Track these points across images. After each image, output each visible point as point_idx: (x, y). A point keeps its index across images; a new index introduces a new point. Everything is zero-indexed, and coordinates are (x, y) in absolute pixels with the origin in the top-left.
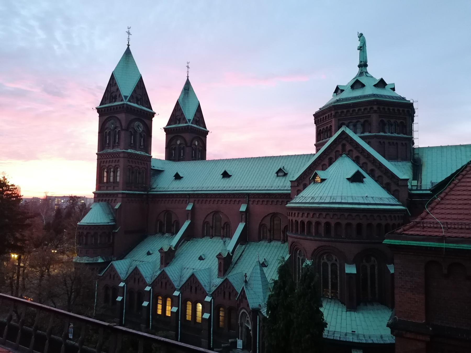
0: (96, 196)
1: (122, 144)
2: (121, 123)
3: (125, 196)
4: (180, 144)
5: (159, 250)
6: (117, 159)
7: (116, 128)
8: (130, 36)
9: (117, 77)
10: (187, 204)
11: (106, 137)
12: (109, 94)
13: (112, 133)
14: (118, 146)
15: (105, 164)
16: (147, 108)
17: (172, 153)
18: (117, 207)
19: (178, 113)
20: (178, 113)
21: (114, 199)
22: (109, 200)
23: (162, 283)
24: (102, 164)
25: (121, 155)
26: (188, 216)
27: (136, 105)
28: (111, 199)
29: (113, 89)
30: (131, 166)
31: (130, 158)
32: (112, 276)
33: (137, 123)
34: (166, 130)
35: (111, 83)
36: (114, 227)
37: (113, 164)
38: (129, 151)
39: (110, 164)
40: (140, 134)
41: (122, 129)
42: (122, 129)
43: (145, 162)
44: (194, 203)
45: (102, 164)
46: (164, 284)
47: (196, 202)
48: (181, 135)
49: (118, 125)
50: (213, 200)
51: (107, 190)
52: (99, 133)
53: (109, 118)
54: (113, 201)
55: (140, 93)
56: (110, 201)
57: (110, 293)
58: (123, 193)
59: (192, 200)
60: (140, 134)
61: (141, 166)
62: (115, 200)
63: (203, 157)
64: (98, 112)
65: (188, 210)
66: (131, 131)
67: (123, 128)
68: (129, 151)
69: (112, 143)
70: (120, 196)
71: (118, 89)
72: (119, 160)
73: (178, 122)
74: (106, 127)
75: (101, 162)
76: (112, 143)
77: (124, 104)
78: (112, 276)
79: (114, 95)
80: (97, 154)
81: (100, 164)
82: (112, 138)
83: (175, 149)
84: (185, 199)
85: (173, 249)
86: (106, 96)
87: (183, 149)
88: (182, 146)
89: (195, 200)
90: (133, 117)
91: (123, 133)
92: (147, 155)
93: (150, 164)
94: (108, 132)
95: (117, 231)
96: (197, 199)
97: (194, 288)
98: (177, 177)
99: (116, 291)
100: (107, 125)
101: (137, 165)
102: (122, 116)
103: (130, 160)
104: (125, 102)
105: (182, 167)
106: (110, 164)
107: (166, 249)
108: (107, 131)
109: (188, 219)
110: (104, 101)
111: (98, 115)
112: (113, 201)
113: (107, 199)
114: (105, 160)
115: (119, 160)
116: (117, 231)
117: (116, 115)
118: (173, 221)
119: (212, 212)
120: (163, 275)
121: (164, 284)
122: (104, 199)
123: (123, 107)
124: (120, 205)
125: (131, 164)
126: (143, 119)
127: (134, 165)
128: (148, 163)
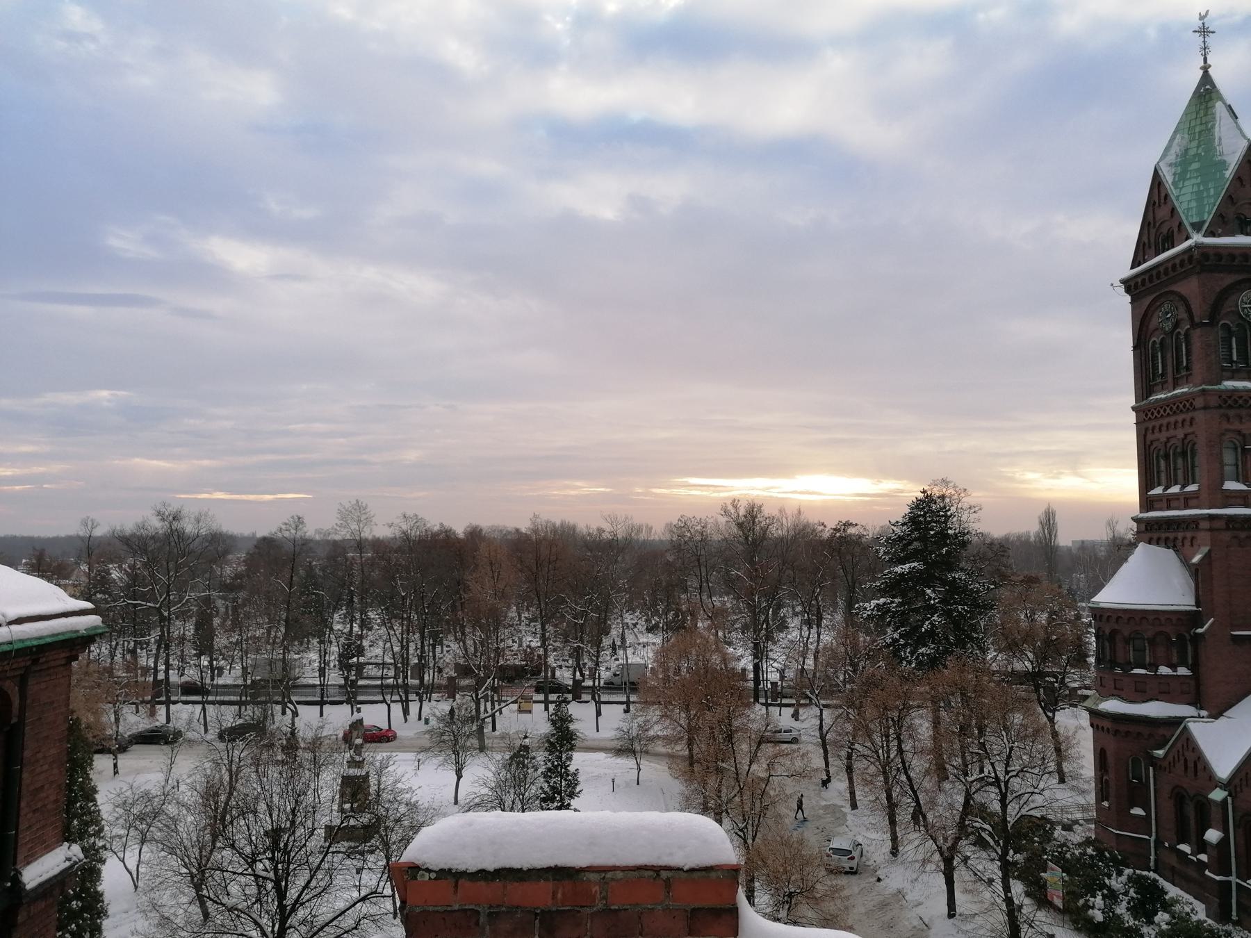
0: (1143, 527)
1: (1197, 368)
2: (1189, 310)
3: (1220, 524)
6: (1187, 416)
7: (1176, 325)
8: (1210, 40)
9: (1168, 177)
11: (1154, 357)
12: (1153, 231)
13: (1168, 341)
14: (1187, 376)
15: (1157, 435)
18: (1196, 559)
21: (1189, 535)
22: (1176, 538)
24: (1150, 437)
25: (1199, 402)
28: (1180, 535)
29: (1163, 213)
30: (1239, 432)
31: (1230, 407)
32: (1191, 765)
36: (1193, 618)
37: (1180, 433)
38: (1229, 384)
41: (1194, 325)
42: (1194, 325)
45: (1150, 437)
49: (1183, 315)
51: (1169, 508)
52: (1135, 348)
53: (1154, 300)
54: (1187, 543)
56: (1179, 543)
57: (1190, 811)
58: (1212, 518)
62: (1193, 538)
64: (1128, 291)
67: (1197, 320)
68: (1229, 384)
69: (1170, 370)
71: (1173, 210)
72: (1192, 419)
75: (1147, 429)
76: (1170, 370)
77: (1198, 246)
78: (1191, 765)
79: (1164, 230)
80: (1133, 408)
81: (1145, 436)
82: (1169, 355)
86: (1145, 239)
90: (1229, 279)
94: (1158, 341)
95: (1200, 630)
100: (1154, 322)
102: (1190, 287)
103: (1231, 413)
104: (1197, 238)
106: (1172, 432)
108: (1156, 339)
110: (1140, 258)
111: (1128, 298)
112: (1187, 543)
113: (1171, 535)
114: (1157, 424)
115: (1192, 419)
116: (1200, 630)
117: (1175, 288)
122: (1163, 535)
124: (1208, 556)
125: (1236, 425)
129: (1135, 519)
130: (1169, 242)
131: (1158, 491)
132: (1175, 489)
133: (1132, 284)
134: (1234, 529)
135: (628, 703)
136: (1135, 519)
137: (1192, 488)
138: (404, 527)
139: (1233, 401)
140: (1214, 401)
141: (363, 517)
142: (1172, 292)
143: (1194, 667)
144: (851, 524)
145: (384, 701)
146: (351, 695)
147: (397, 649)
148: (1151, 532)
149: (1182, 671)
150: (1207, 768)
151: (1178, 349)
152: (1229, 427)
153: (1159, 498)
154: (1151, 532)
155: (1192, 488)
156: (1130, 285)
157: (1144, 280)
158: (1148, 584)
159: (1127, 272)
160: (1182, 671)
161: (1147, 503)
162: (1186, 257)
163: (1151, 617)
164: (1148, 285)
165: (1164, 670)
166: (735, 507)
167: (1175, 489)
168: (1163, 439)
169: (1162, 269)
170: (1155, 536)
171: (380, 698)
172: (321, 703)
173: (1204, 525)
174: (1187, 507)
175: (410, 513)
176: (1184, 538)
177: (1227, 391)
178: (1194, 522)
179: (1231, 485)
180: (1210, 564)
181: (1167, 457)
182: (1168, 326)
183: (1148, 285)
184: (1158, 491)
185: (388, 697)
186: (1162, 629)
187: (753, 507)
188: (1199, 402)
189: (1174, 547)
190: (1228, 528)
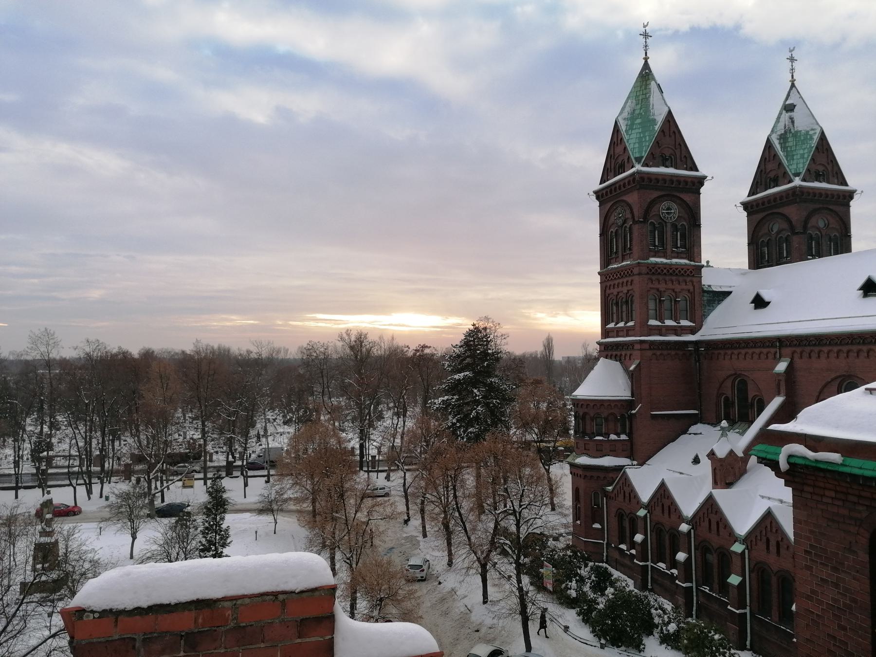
1: (636, 249)
3: (647, 346)
4: (778, 233)
5: (708, 456)
6: (630, 279)
7: (625, 222)
9: (623, 127)
10: (777, 361)
13: (620, 232)
15: (612, 290)
16: (686, 169)
17: (764, 252)
18: (632, 368)
19: (770, 166)
20: (770, 166)
21: (628, 353)
22: (621, 355)
23: (710, 521)
25: (636, 271)
26: (779, 385)
27: (671, 171)
28: (623, 353)
29: (619, 150)
30: (658, 290)
32: (627, 495)
33: (665, 204)
34: (746, 206)
35: (615, 140)
36: (629, 404)
37: (625, 289)
38: (653, 260)
39: (620, 289)
40: (675, 227)
41: (635, 222)
43: (688, 279)
44: (792, 359)
45: (608, 291)
46: (714, 526)
47: (796, 356)
48: (780, 210)
49: (629, 216)
50: (835, 349)
51: (618, 336)
52: (601, 235)
54: (628, 358)
55: (670, 143)
57: (627, 524)
58: (642, 342)
59: (787, 351)
60: (675, 227)
61: (678, 288)
63: (850, 251)
64: (598, 198)
65: (778, 374)
66: (652, 224)
67: (636, 219)
68: (653, 260)
69: (620, 250)
70: (637, 346)
71: (625, 148)
73: (772, 184)
74: (611, 222)
76: (620, 250)
78: (627, 495)
79: (620, 160)
80: (599, 273)
83: (768, 244)
84: (773, 350)
85: (740, 454)
87: (787, 240)
88: (784, 235)
89: (794, 353)
90: (656, 194)
91: (636, 228)
92: (692, 263)
93: (700, 281)
95: (633, 412)
96: (799, 350)
97: (773, 543)
98: (759, 302)
99: (634, 525)
100: (612, 219)
101: (670, 285)
102: (633, 198)
103: (654, 278)
104: (638, 167)
105: (777, 281)
106: (620, 289)
107: (721, 453)
108: (613, 230)
109: (779, 394)
111: (598, 203)
112: (628, 358)
113: (619, 353)
116: (633, 412)
118: (750, 397)
119: (840, 376)
120: (710, 504)
121: (714, 526)
122: (614, 353)
123: (634, 179)
124: (639, 365)
125: (656, 285)
126: (678, 194)
127: (662, 287)
128: (695, 279)
129: (598, 343)
130: (622, 168)
131: (612, 325)
132: (621, 324)
133: (600, 194)
134: (654, 349)
135: (268, 476)
136: (598, 343)
137: (631, 324)
138: (88, 350)
139: (655, 270)
140: (644, 270)
141: (51, 342)
142: (623, 201)
143: (630, 435)
144: (427, 347)
145: (71, 485)
146: (42, 481)
147: (81, 444)
148: (608, 350)
149: (623, 437)
150: (636, 496)
151: (625, 236)
152: (652, 286)
153: (612, 329)
154: (608, 350)
155: (631, 324)
156: (599, 195)
157: (607, 192)
158: (605, 383)
159: (597, 186)
160: (623, 437)
161: (606, 333)
162: (631, 179)
163: (606, 404)
164: (609, 195)
165: (613, 437)
166: (348, 335)
167: (621, 324)
168: (615, 293)
169: (617, 186)
170: (610, 353)
171: (67, 482)
172: (16, 489)
173: (637, 346)
174: (628, 335)
175: (92, 338)
176: (626, 355)
177: (652, 264)
178: (631, 344)
179: (653, 322)
180: (640, 370)
181: (617, 304)
182: (620, 222)
183: (609, 195)
184: (612, 325)
185: (74, 482)
186: (612, 411)
187: (361, 335)
188: (636, 271)
189: (620, 361)
190: (650, 349)
